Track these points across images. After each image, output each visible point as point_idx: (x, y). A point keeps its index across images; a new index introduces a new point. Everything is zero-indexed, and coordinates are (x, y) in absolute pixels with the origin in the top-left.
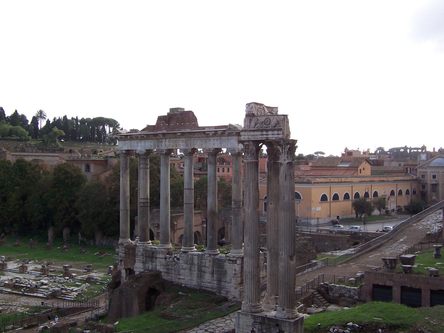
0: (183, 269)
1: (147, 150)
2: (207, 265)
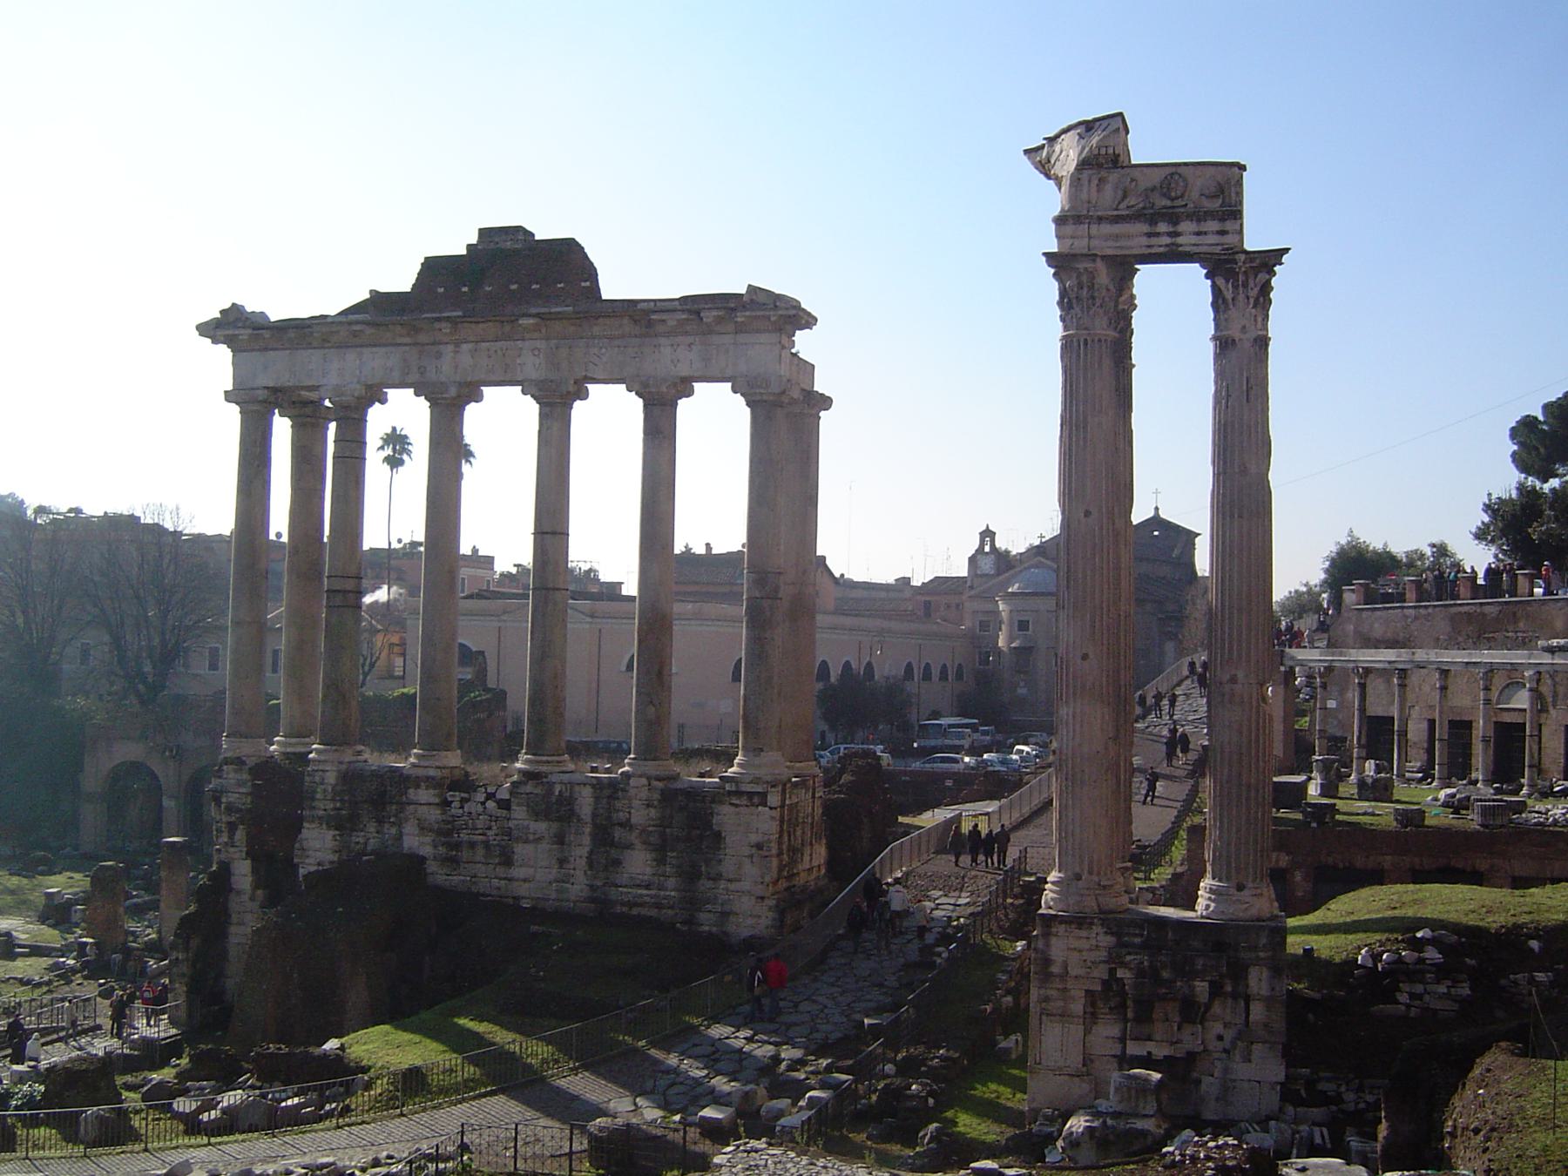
0: (527, 841)
1: (369, 387)
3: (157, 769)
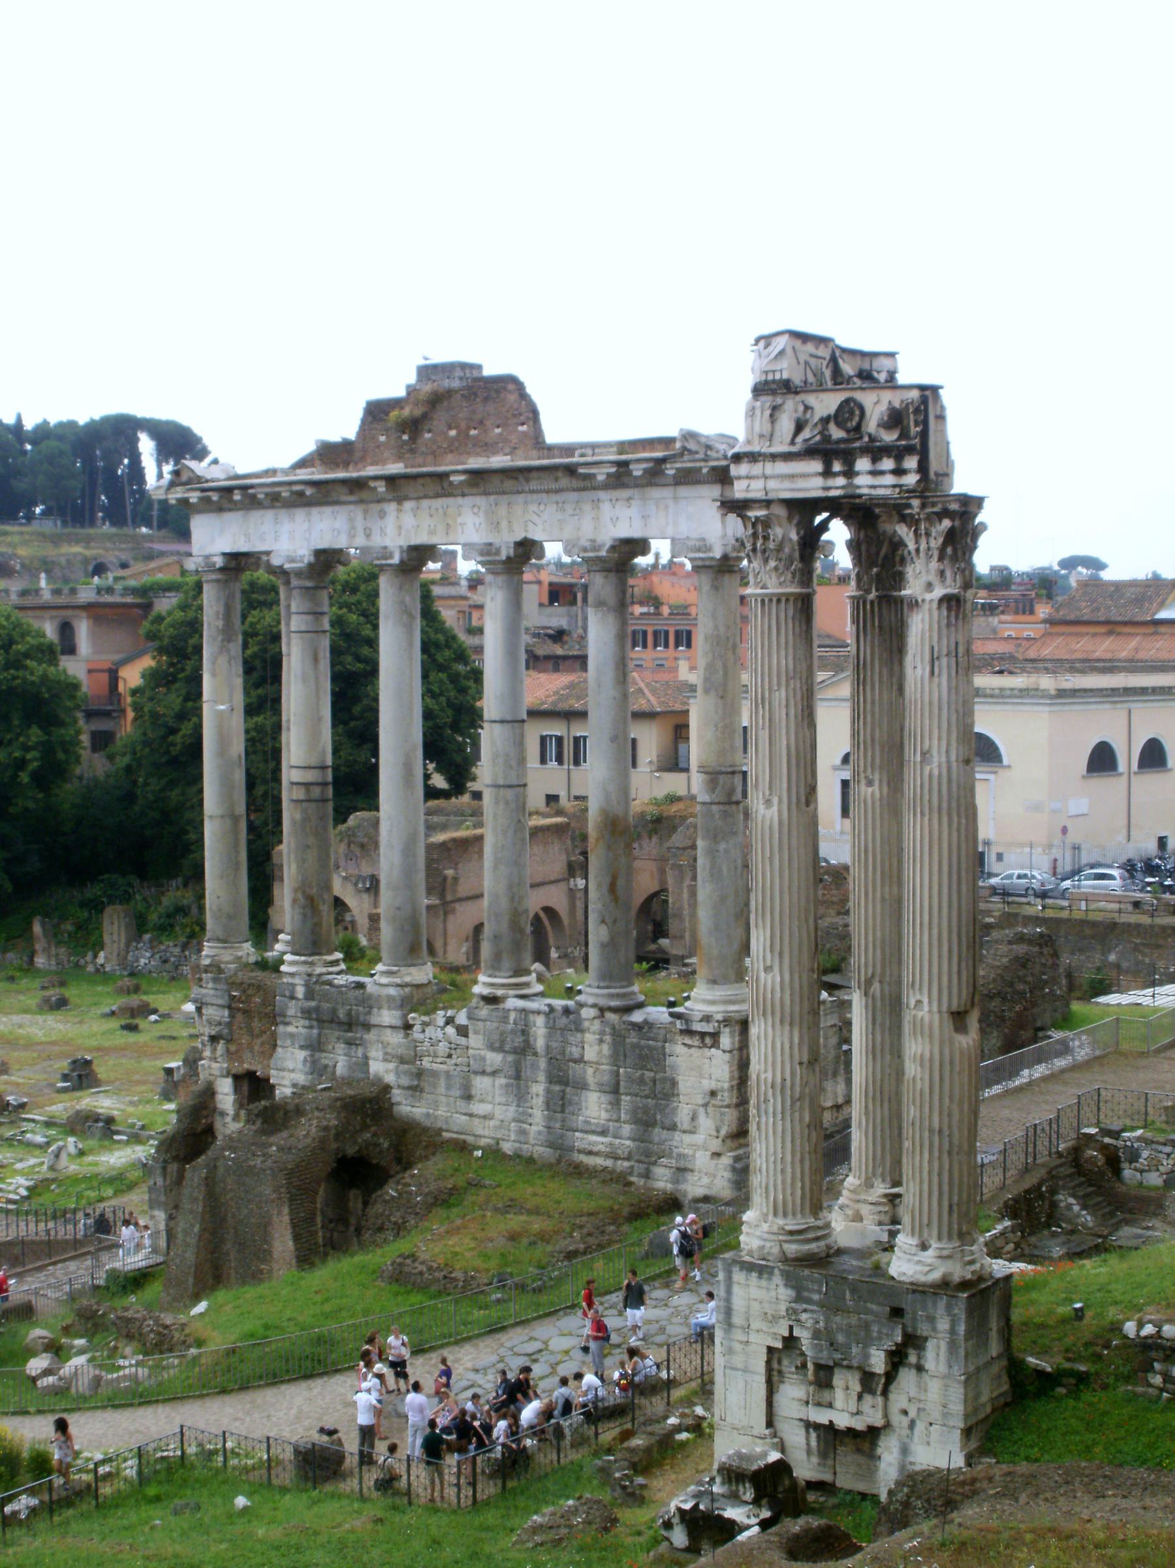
0: (483, 1073)
1: (319, 553)
2: (590, 1054)
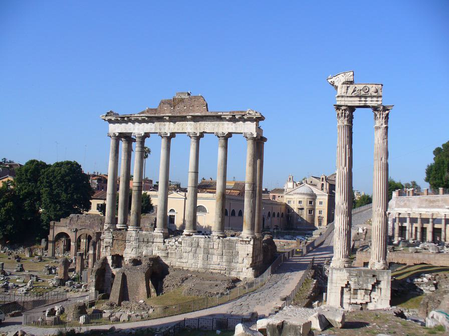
1: (145, 133)
3: (69, 234)
